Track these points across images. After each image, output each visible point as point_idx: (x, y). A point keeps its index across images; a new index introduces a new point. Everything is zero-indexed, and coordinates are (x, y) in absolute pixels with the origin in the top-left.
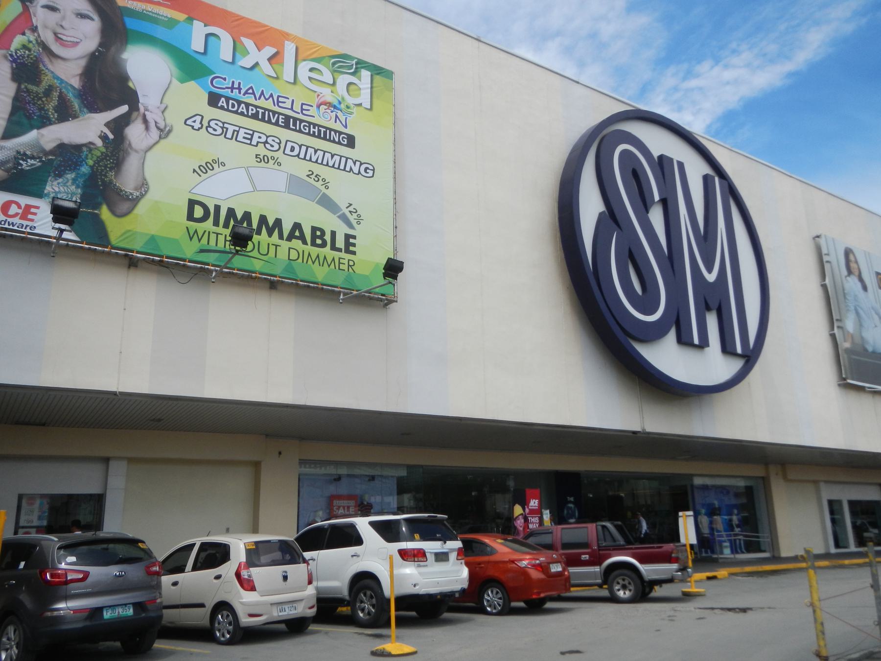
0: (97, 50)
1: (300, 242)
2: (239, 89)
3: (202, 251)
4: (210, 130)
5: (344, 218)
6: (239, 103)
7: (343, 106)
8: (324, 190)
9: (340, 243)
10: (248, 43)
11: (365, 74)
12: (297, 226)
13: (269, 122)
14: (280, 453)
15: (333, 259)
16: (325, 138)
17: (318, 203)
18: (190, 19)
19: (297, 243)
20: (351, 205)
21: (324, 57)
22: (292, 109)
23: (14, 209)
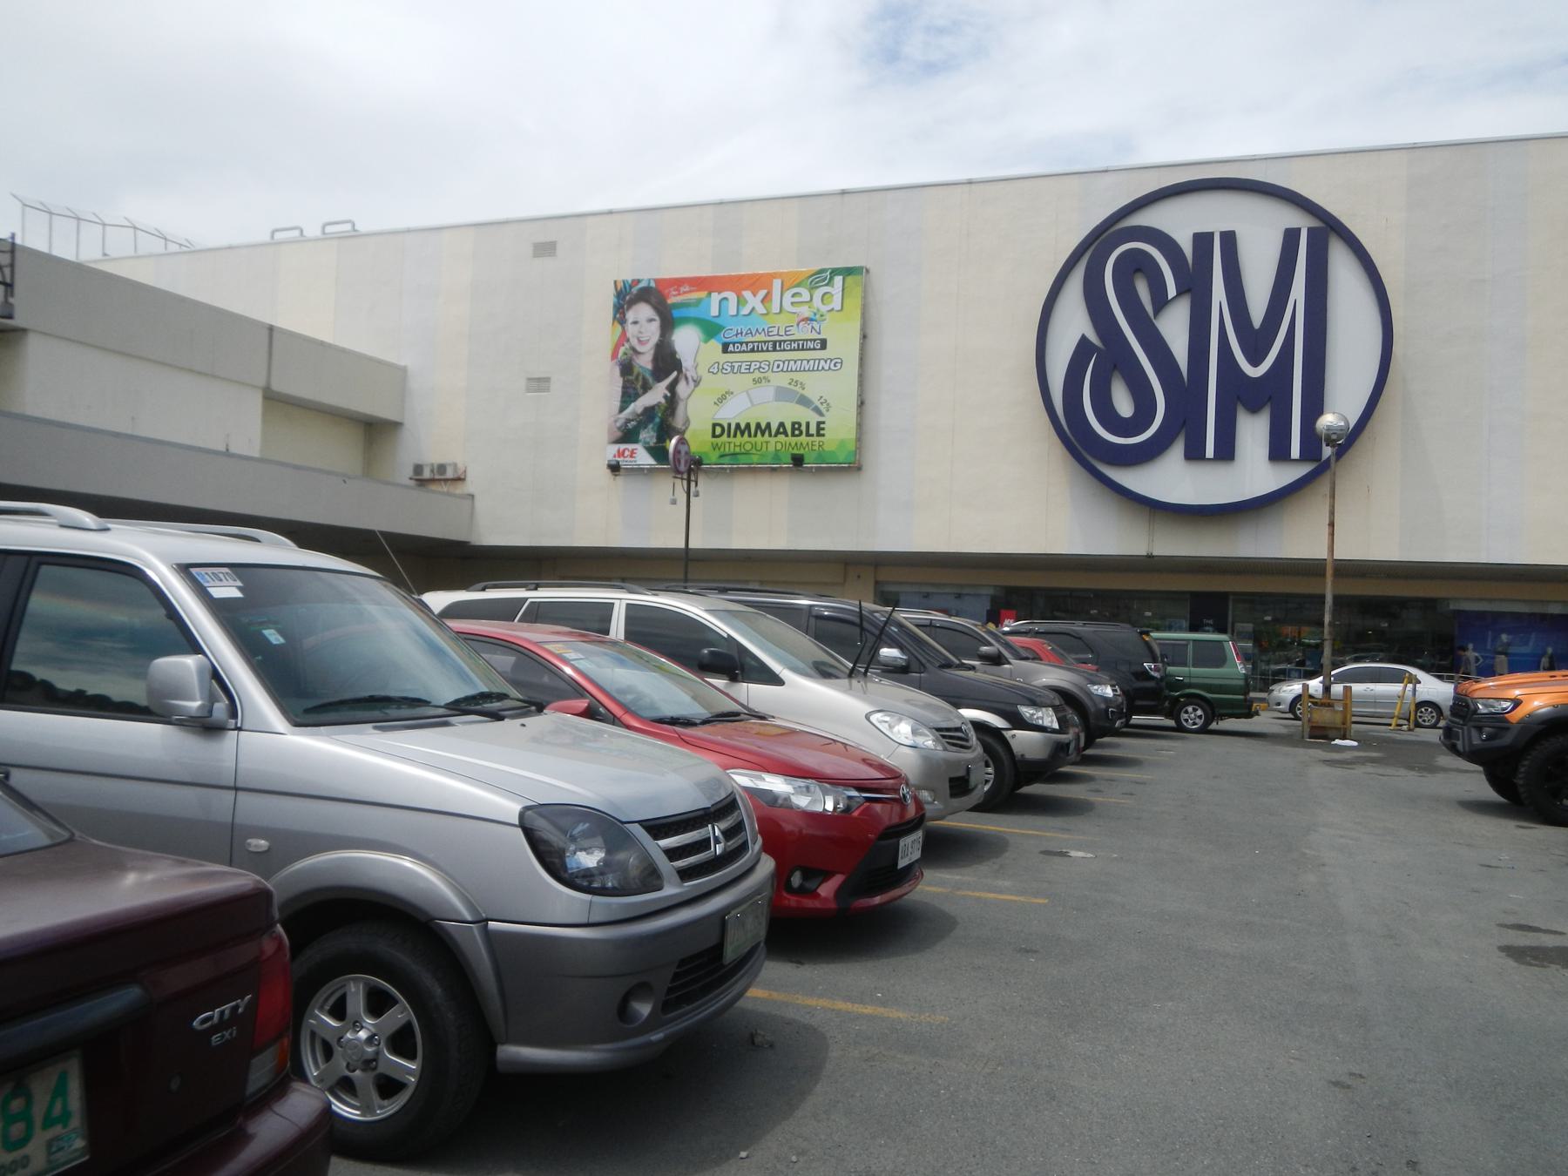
0: (660, 340)
1: (783, 436)
2: (741, 333)
3: (722, 456)
4: (724, 371)
5: (818, 411)
6: (741, 343)
7: (818, 316)
8: (801, 391)
9: (813, 430)
10: (747, 294)
11: (838, 280)
12: (782, 425)
13: (762, 351)
14: (859, 577)
15: (808, 444)
16: (803, 349)
17: (797, 403)
18: (710, 294)
19: (781, 438)
20: (821, 397)
21: (803, 281)
22: (778, 335)
23: (627, 453)
